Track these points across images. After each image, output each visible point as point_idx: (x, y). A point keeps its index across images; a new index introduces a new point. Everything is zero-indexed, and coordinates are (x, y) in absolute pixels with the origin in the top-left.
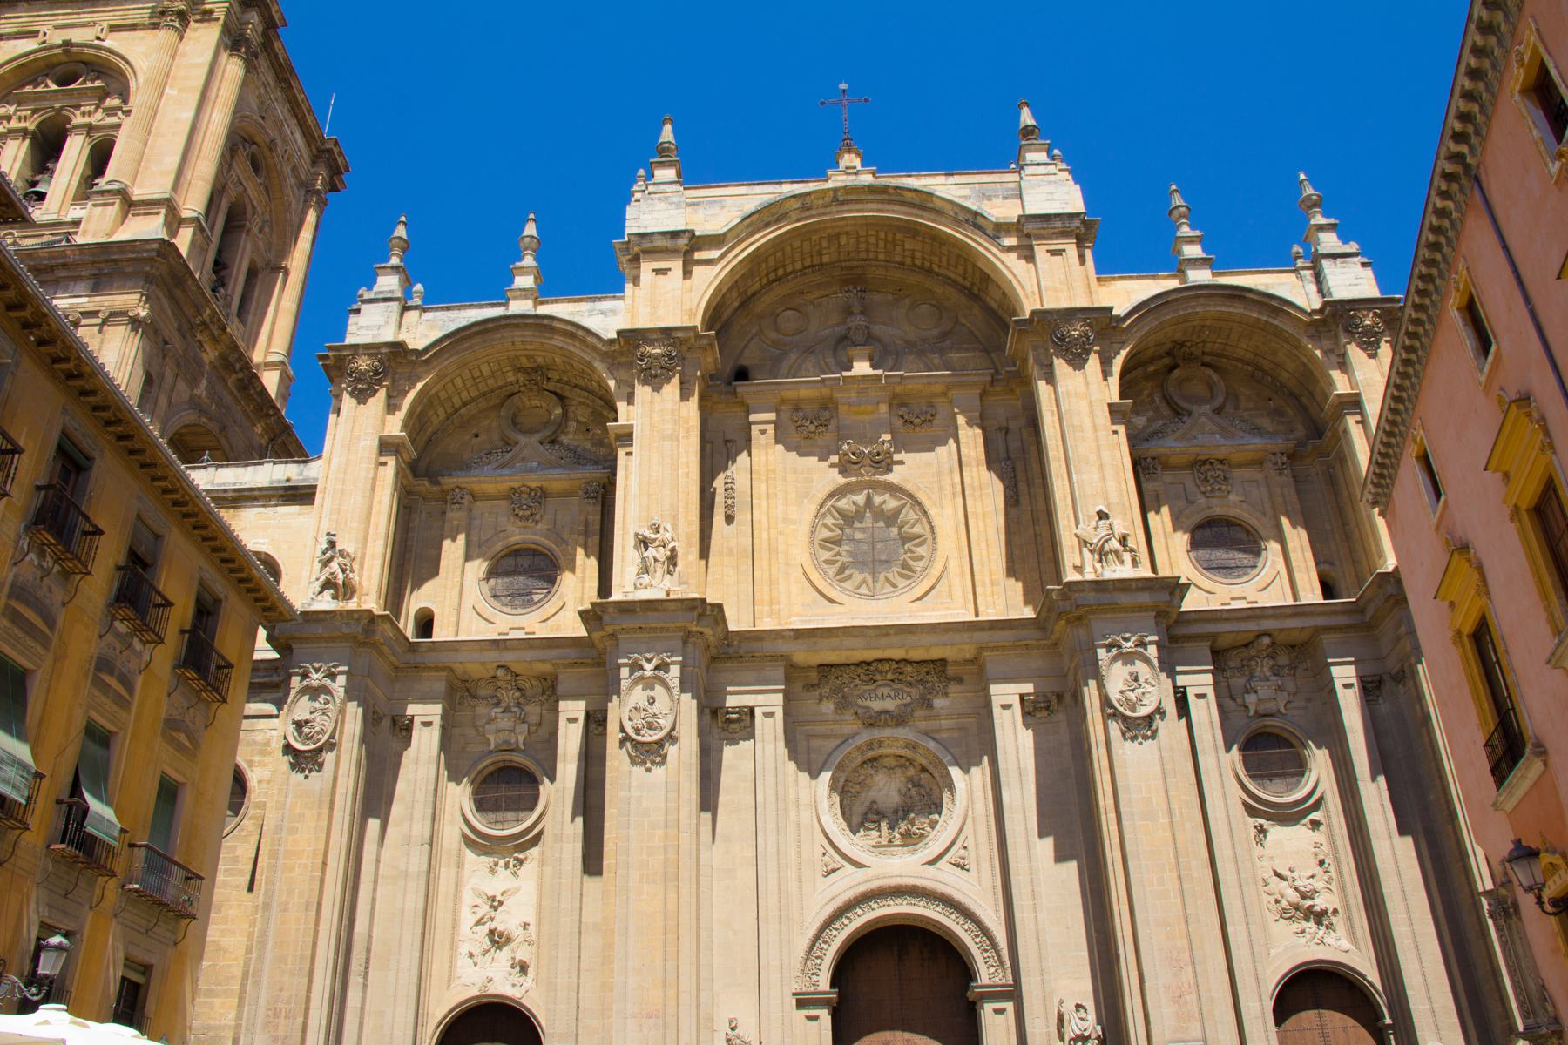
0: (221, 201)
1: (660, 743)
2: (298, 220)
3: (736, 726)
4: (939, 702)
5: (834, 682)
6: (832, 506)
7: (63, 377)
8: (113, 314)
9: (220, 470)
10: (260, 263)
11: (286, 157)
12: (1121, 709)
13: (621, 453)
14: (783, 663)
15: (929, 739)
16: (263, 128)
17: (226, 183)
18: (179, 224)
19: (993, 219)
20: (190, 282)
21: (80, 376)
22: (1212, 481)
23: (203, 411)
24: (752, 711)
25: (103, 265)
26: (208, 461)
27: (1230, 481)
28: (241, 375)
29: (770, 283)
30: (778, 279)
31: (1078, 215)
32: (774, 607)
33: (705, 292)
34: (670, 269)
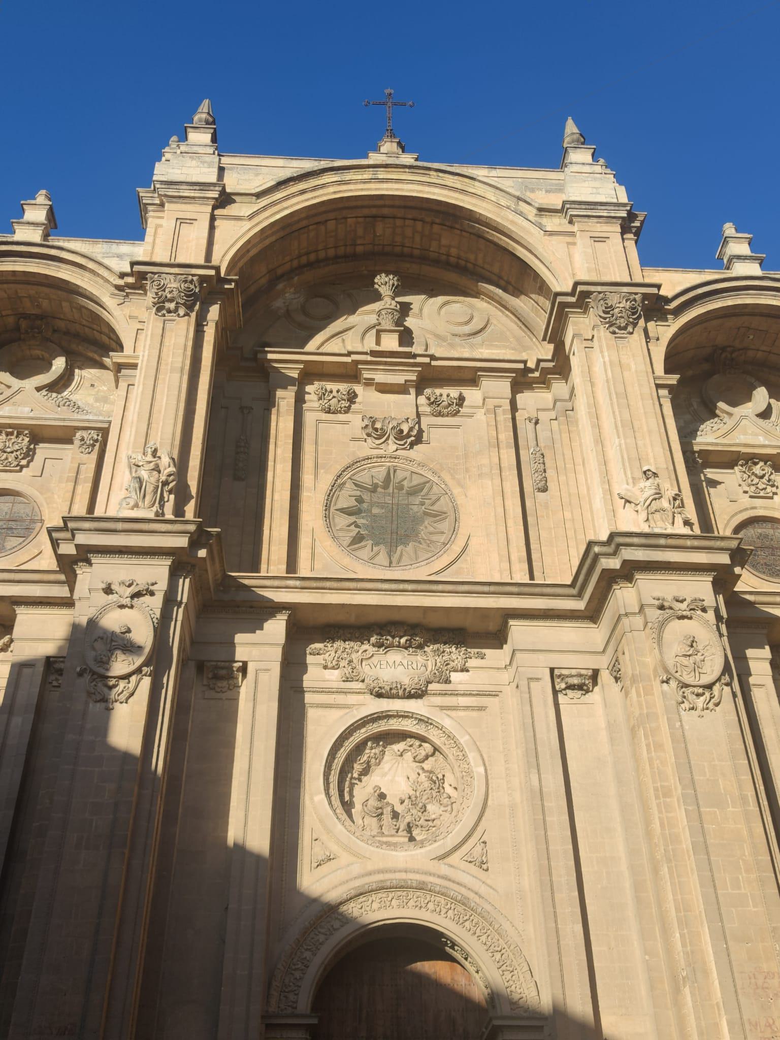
1: (127, 677)
3: (224, 683)
4: (455, 677)
5: (339, 644)
6: (350, 478)
12: (677, 675)
13: (123, 385)
14: (286, 618)
15: (445, 716)
19: (537, 205)
22: (756, 480)
24: (245, 664)
27: (775, 483)
29: (301, 268)
30: (310, 265)
31: (624, 205)
32: (280, 567)
33: (232, 246)
34: (196, 220)
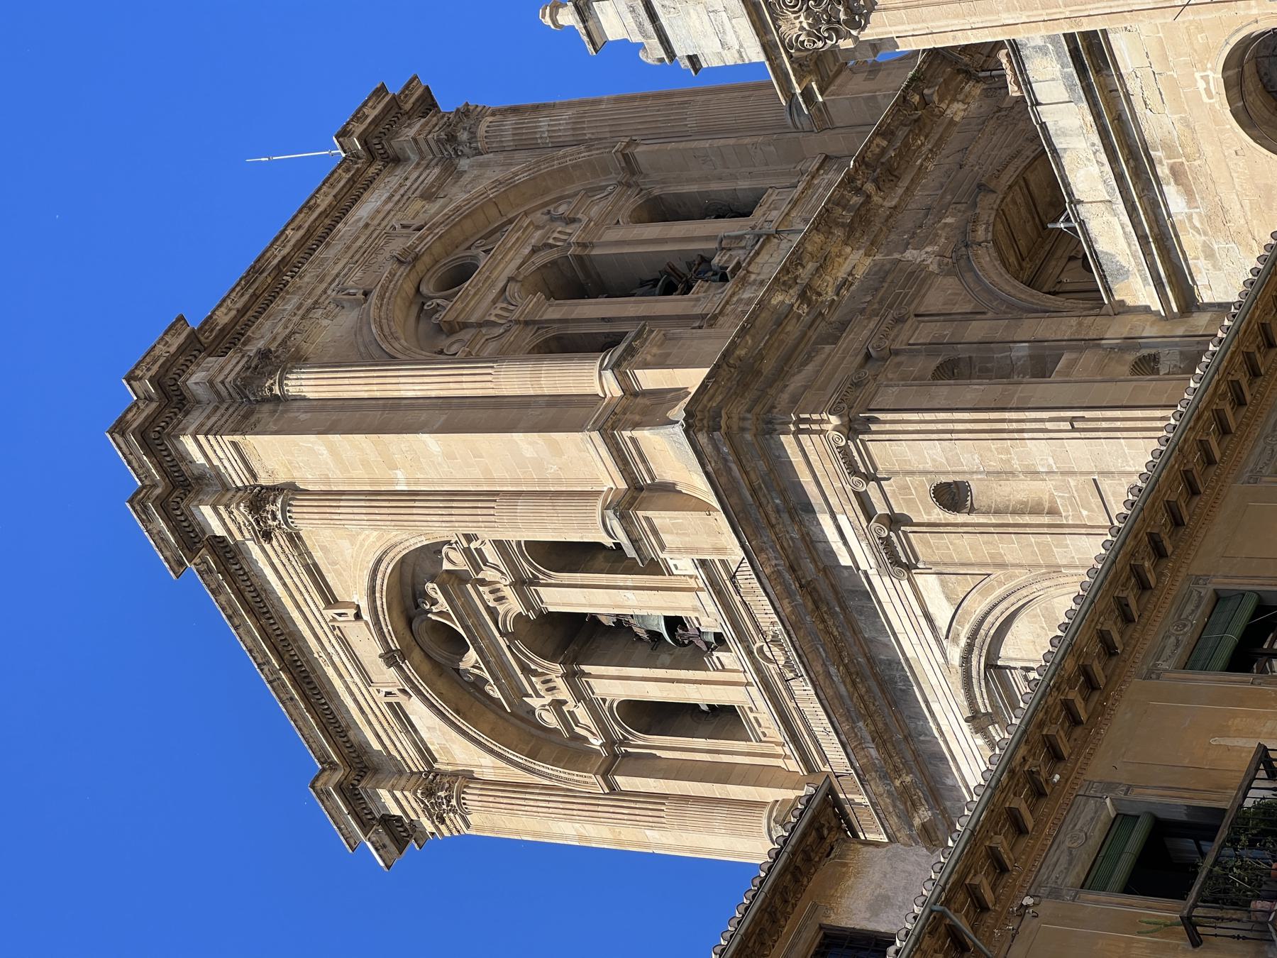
0: (554, 321)
2: (519, 156)
7: (1096, 696)
8: (854, 471)
9: (1077, 196)
10: (632, 201)
11: (417, 223)
16: (385, 289)
17: (517, 322)
18: (636, 394)
20: (741, 352)
21: (1085, 671)
23: (965, 242)
25: (769, 509)
26: (1068, 220)
28: (870, 187)
